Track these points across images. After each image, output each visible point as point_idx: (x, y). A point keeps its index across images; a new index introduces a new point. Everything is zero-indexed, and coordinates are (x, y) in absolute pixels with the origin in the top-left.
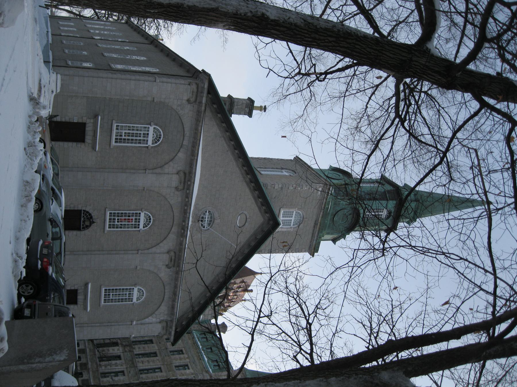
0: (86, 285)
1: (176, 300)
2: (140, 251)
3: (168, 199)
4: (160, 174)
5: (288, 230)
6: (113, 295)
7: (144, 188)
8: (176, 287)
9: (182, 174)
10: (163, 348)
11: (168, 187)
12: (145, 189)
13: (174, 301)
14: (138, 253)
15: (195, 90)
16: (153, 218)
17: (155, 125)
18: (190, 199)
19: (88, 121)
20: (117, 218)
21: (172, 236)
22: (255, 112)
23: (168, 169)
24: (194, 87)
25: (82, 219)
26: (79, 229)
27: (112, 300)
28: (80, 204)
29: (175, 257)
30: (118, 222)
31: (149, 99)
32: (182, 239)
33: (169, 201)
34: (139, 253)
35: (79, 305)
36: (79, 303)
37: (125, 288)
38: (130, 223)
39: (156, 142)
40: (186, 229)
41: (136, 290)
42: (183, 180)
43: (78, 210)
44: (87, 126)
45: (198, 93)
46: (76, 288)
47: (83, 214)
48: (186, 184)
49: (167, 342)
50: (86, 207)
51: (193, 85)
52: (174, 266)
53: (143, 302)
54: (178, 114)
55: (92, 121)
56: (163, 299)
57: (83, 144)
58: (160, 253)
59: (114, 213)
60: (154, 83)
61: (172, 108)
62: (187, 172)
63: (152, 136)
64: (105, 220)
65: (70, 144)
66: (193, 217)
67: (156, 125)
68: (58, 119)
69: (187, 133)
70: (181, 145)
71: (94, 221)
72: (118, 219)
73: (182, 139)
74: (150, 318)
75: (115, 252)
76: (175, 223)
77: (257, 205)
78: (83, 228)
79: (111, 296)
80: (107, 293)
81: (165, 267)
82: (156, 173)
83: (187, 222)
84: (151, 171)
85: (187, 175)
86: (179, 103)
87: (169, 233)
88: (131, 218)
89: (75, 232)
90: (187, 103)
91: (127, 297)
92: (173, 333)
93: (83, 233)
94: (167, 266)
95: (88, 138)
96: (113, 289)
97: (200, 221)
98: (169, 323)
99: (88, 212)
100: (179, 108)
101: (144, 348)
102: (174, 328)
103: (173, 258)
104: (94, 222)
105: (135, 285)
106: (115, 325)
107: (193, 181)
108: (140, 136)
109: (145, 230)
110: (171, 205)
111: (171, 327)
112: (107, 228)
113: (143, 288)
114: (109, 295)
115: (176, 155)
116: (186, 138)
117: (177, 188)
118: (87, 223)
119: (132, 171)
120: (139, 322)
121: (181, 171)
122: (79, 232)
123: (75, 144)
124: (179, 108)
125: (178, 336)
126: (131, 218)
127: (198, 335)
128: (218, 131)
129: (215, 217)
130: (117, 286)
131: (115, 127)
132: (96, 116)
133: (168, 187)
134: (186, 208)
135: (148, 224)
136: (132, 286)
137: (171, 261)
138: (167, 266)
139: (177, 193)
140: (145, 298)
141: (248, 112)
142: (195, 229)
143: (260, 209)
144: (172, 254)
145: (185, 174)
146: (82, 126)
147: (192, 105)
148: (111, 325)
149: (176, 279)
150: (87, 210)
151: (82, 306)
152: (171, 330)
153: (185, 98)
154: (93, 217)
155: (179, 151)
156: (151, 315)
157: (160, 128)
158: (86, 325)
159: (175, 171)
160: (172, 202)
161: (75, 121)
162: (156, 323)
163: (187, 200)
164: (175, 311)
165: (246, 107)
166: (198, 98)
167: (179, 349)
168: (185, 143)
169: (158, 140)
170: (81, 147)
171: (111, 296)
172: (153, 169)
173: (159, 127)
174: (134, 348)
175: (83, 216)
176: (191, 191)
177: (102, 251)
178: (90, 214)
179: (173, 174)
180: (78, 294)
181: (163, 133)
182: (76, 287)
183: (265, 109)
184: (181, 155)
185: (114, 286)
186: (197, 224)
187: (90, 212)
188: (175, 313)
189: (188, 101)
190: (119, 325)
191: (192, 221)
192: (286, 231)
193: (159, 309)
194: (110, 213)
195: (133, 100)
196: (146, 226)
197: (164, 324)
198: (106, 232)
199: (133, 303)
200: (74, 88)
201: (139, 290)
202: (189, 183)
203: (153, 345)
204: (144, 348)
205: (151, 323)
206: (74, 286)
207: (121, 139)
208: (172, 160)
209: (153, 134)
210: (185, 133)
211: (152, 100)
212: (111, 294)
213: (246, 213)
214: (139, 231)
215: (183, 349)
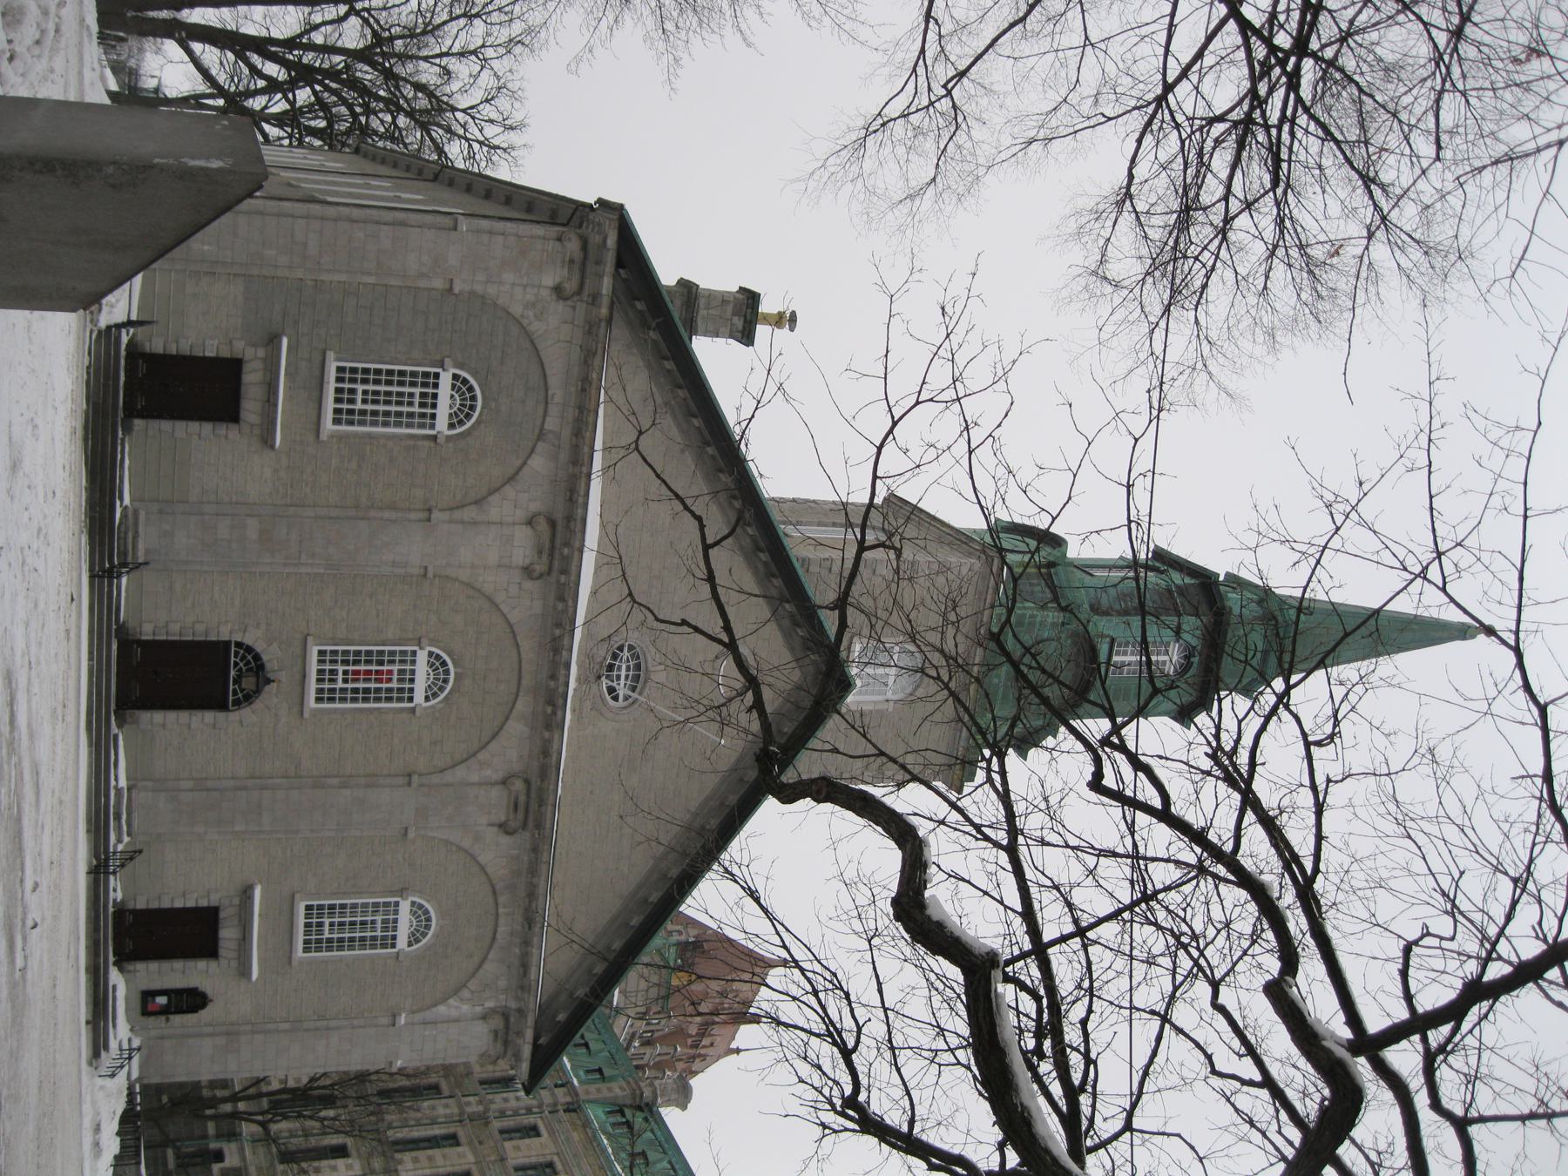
0: (246, 893)
1: (535, 940)
2: (415, 779)
4: (475, 523)
5: (879, 707)
6: (332, 924)
7: (426, 568)
8: (532, 895)
9: (543, 526)
10: (493, 1158)
11: (499, 566)
12: (430, 574)
13: (526, 943)
15: (578, 255)
16: (455, 666)
17: (456, 366)
18: (570, 603)
19: (249, 353)
20: (341, 669)
21: (516, 728)
22: (762, 331)
23: (500, 508)
24: (573, 246)
25: (232, 673)
26: (222, 706)
27: (330, 941)
28: (227, 622)
30: (345, 681)
31: (438, 284)
32: (547, 735)
33: (503, 607)
35: (223, 962)
36: (222, 952)
37: (371, 901)
38: (384, 686)
39: (461, 423)
40: (561, 701)
41: (405, 907)
42: (547, 545)
43: (218, 643)
44: (246, 368)
45: (584, 263)
46: (213, 904)
47: (236, 656)
48: (557, 556)
49: (504, 1140)
50: (245, 631)
51: (570, 240)
52: (524, 826)
53: (428, 947)
54: (526, 332)
55: (261, 353)
56: (494, 939)
57: (233, 427)
58: (480, 784)
59: (334, 653)
60: (453, 233)
61: (508, 313)
62: (559, 517)
63: (449, 401)
64: (304, 676)
65: (194, 426)
66: (580, 666)
67: (461, 367)
68: (157, 346)
69: (557, 393)
70: (537, 431)
71: (271, 676)
72: (345, 673)
73: (540, 412)
74: (451, 1001)
75: (335, 781)
78: (237, 703)
79: (327, 928)
80: (314, 920)
82: (462, 522)
83: (562, 679)
84: (445, 516)
85: (559, 528)
86: (528, 297)
87: (507, 718)
88: (385, 668)
89: (209, 716)
90: (554, 297)
91: (379, 933)
92: (527, 1051)
93: (234, 716)
95: (250, 408)
96: (332, 907)
97: (603, 678)
98: (512, 1020)
99: (249, 649)
100: (531, 313)
101: (430, 1158)
102: (529, 1034)
103: (522, 799)
104: (269, 681)
105: (402, 892)
106: (338, 1028)
107: (577, 544)
108: (410, 404)
109: (432, 707)
110: (511, 626)
111: (520, 1034)
112: (311, 702)
113: (428, 901)
114: (320, 925)
115: (525, 463)
116: (554, 410)
117: (527, 571)
118: (249, 683)
119: (387, 514)
120: (418, 1017)
121: (540, 514)
122: (221, 715)
123: (207, 427)
124: (531, 313)
125: (544, 1060)
126: (385, 668)
127: (603, 1117)
129: (650, 665)
130: (346, 894)
131: (332, 374)
132: (273, 341)
133: (499, 566)
134: (557, 632)
135: (442, 689)
136: (393, 893)
138: (500, 826)
139: (528, 585)
140: (436, 936)
141: (740, 328)
142: (588, 704)
143: (787, 636)
144: (519, 785)
145: (552, 524)
146: (233, 367)
147: (569, 303)
148: (328, 1029)
149: (533, 871)
150: (248, 640)
151: (234, 964)
152: (520, 1041)
153: (549, 280)
154: (268, 666)
155: (532, 451)
156: (456, 991)
157: (473, 375)
158: (249, 1028)
159: (520, 514)
161: (210, 353)
162: (473, 1019)
163: (560, 606)
164: (533, 977)
165: (734, 314)
166: (587, 281)
167: (542, 1160)
168: (551, 424)
169: (468, 416)
170: (226, 437)
171: (327, 928)
172: (451, 509)
173: (469, 373)
174: (400, 1162)
175: (236, 664)
176: (573, 578)
177: (296, 777)
178: (257, 657)
179: (514, 524)
181: (483, 393)
182: (214, 900)
183: (793, 319)
184: (538, 463)
185: (335, 895)
186: (594, 687)
187: (259, 649)
188: (533, 987)
189: (558, 290)
190: (353, 1027)
191: (578, 679)
192: (871, 712)
194: (321, 653)
195: (386, 286)
196: (435, 695)
197: (497, 1022)
198: (306, 715)
199: (398, 953)
200: (206, 248)
202: (566, 551)
203: (459, 1149)
204: (430, 1158)
205: (456, 1020)
206: (208, 896)
207: (351, 412)
208: (511, 479)
209: (452, 396)
210: (550, 392)
211: (447, 287)
212: (327, 921)
214: (413, 710)
215: (556, 1159)
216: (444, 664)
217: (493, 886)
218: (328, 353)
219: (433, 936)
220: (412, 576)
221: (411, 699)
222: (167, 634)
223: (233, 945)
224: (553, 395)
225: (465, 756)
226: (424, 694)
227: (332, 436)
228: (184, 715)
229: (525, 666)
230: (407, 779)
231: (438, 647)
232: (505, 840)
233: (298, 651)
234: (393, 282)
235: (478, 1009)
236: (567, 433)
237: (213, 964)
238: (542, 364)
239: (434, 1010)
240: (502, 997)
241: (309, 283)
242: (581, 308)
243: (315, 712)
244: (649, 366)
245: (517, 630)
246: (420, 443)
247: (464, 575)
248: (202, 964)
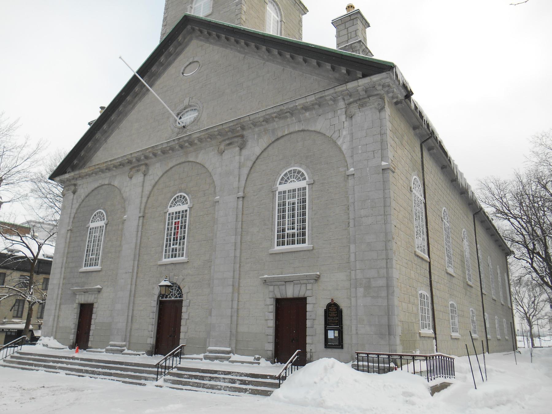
16: (177, 194)
17: (89, 223)
19: (77, 302)
25: (173, 299)
29: (224, 140)
33: (156, 180)
36: (301, 295)
56: (303, 131)
57: (95, 306)
65: (93, 322)
74: (339, 143)
76: (183, 160)
77: (174, 60)
89: (184, 309)
93: (184, 297)
94: (242, 147)
120: (349, 160)
122: (184, 303)
123: (94, 316)
128: (101, 149)
130: (273, 224)
138: (241, 149)
139: (150, 172)
144: (222, 147)
151: (309, 287)
155: (114, 185)
160: (160, 174)
170: (97, 308)
176: (140, 154)
180: (285, 297)
185: (272, 230)
193: (322, 131)
195: (68, 253)
197: (354, 109)
201: (284, 181)
209: (96, 222)
216: (175, 199)
217: (273, 142)
218: (80, 271)
219: (300, 167)
222: (152, 331)
223: (297, 288)
224: (100, 184)
227: (101, 266)
228: (183, 322)
229: (178, 162)
232: (250, 144)
233: (164, 268)
234: (66, 251)
235: (346, 124)
236: (108, 174)
237: (309, 300)
238: (93, 191)
239: (345, 152)
240: (339, 112)
241: (64, 281)
242: (79, 182)
243: (187, 256)
244: (95, 152)
245: (165, 170)
246: (107, 230)
247: (144, 200)
248: (309, 308)
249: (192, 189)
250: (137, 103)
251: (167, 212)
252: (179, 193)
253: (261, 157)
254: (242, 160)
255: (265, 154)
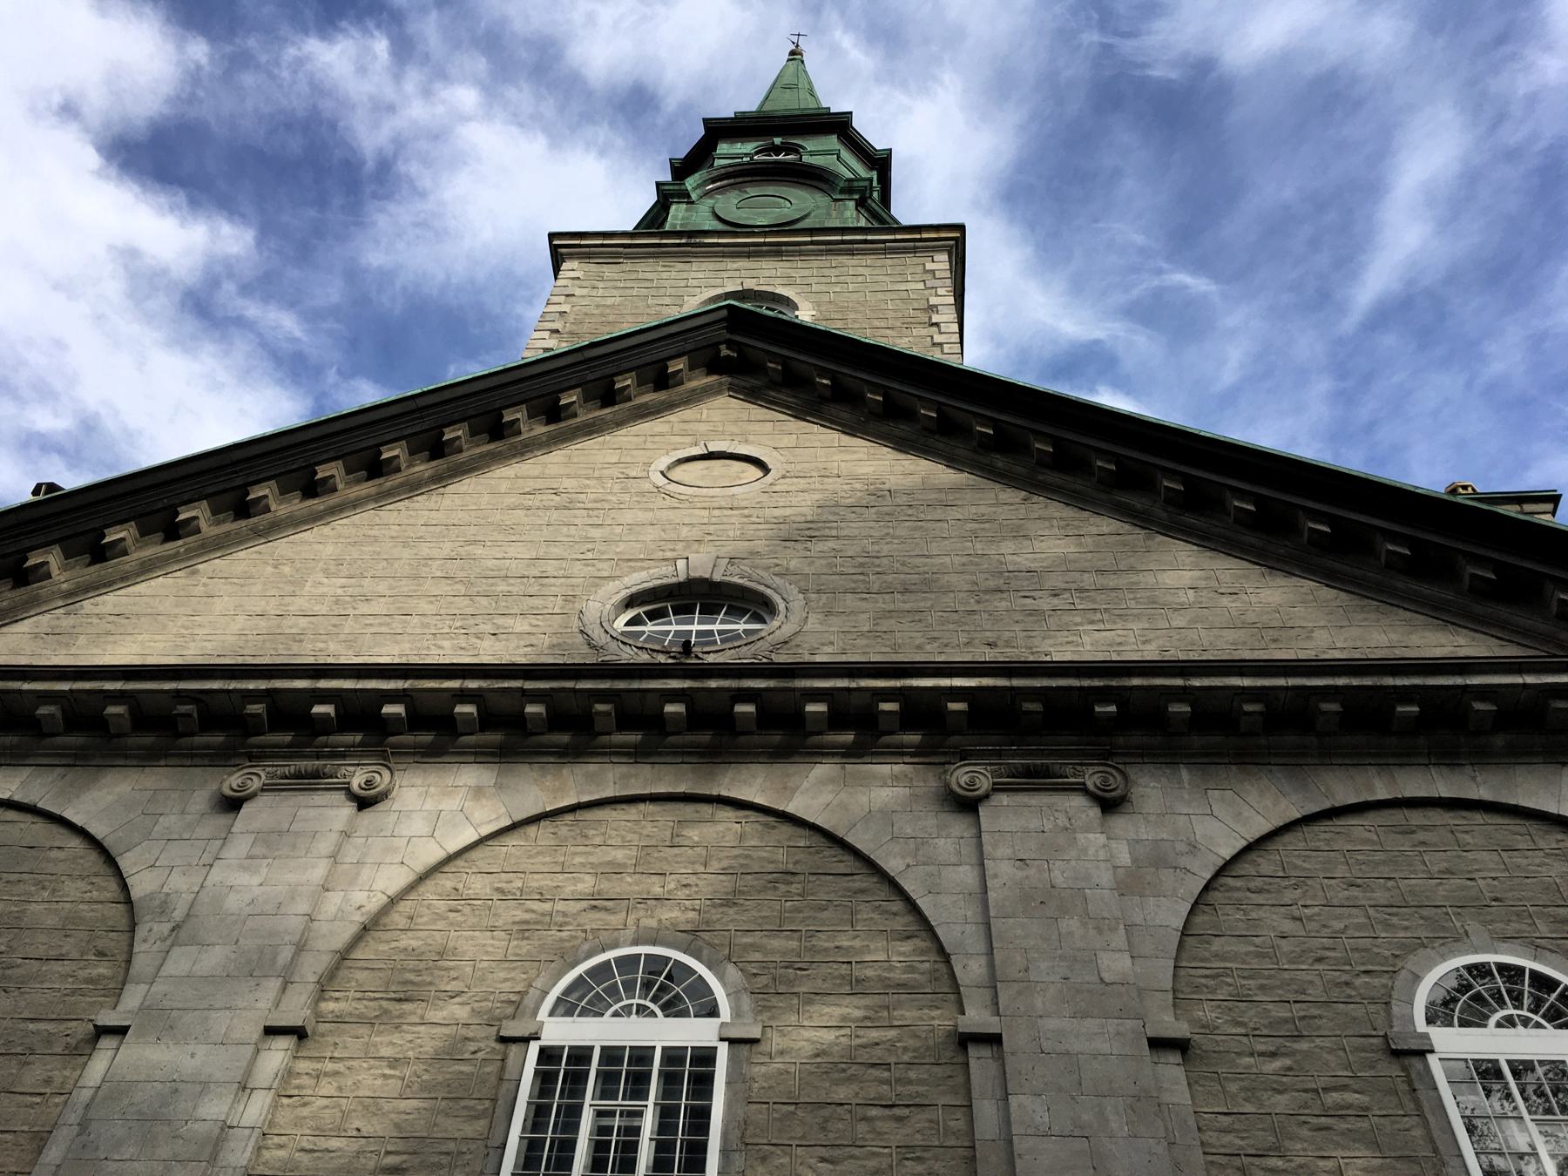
2: (976, 1018)
3: (454, 845)
14: (994, 1040)
16: (615, 945)
34: (989, 1024)
77: (620, 424)
81: (1119, 823)
110: (514, 827)
128: (24, 627)
137: (1045, 772)
196: (702, 987)
213: (664, 462)
219: (1535, 959)
220: (289, 1074)
221: (705, 1057)
225: (898, 906)
226: (693, 1020)
230: (973, 1051)
231: (545, 993)
249: (747, 939)
250: (355, 505)
251: (526, 1040)
252: (636, 943)
253: (1245, 868)
254: (1124, 858)
255: (1266, 863)
